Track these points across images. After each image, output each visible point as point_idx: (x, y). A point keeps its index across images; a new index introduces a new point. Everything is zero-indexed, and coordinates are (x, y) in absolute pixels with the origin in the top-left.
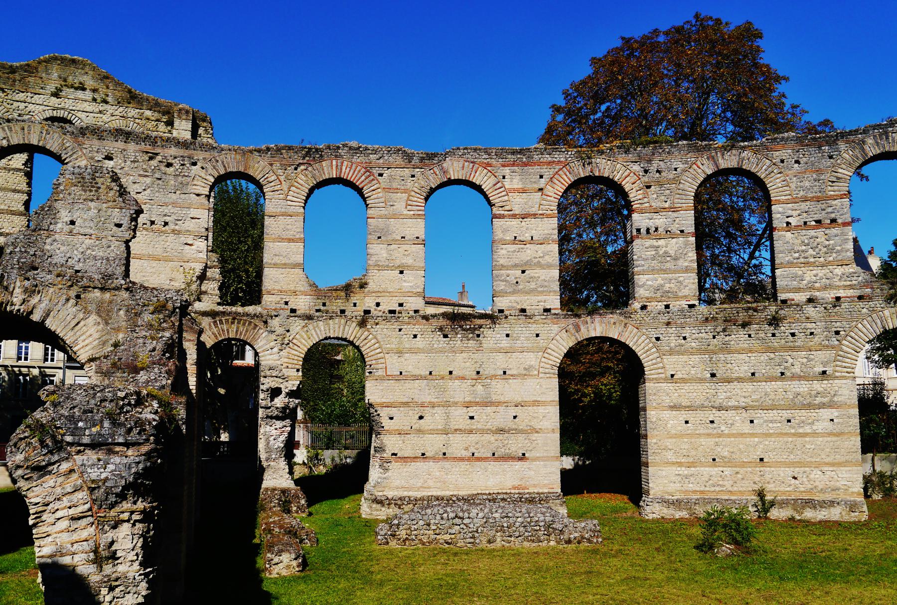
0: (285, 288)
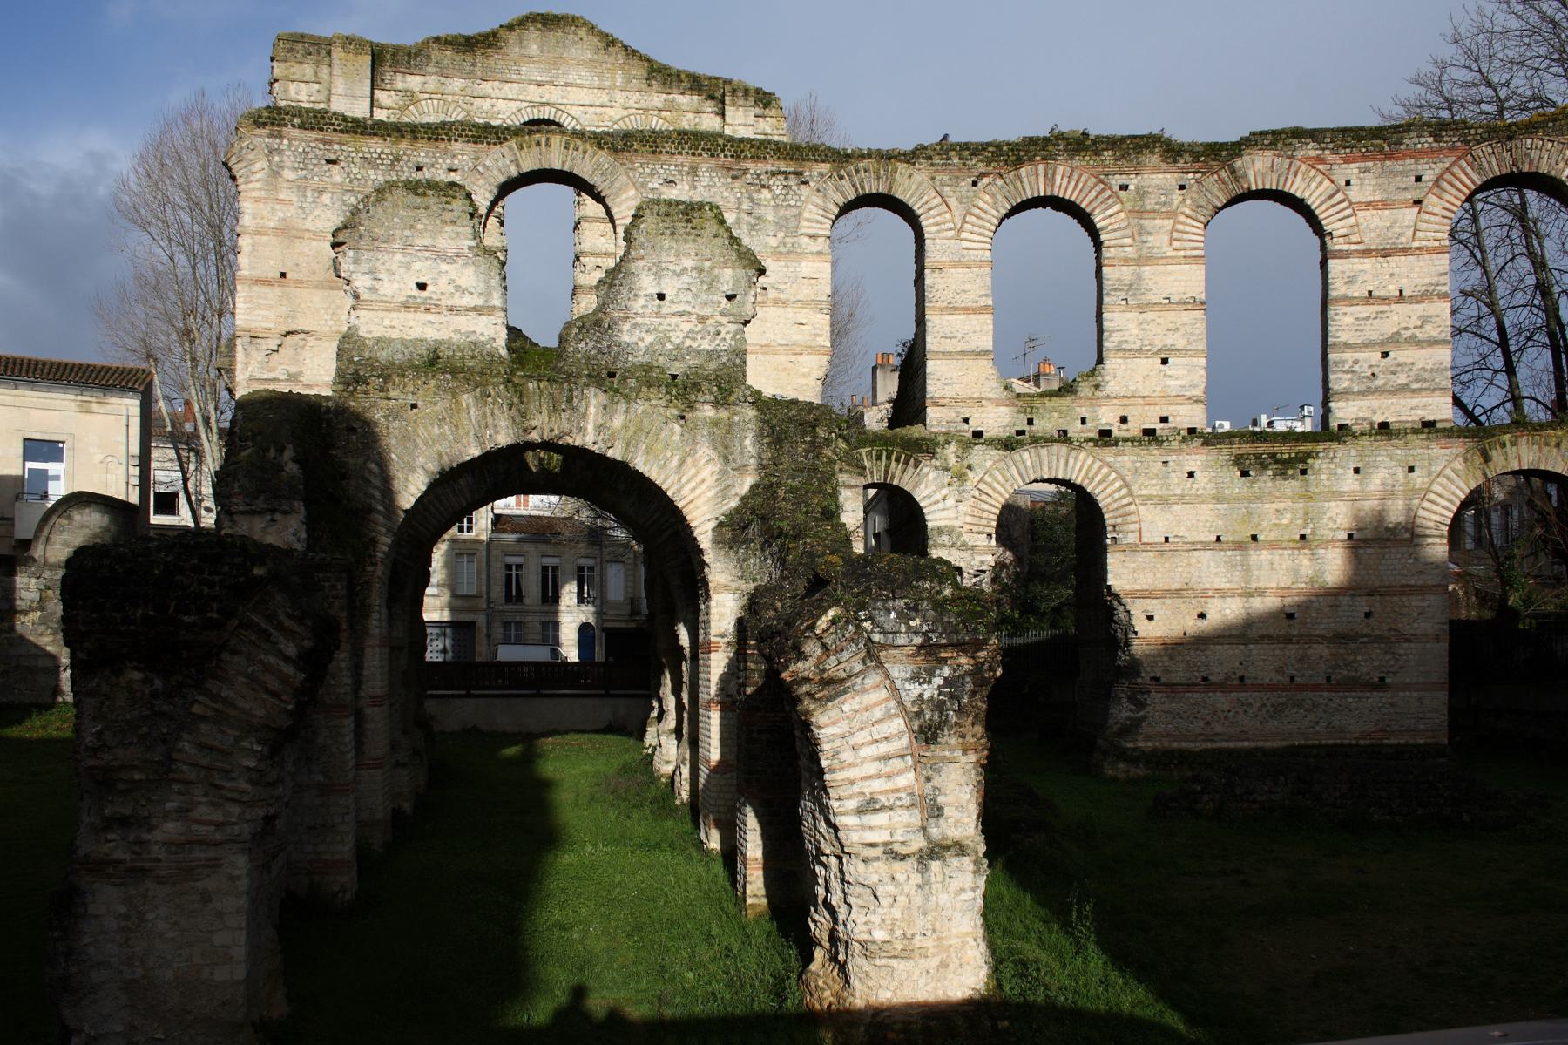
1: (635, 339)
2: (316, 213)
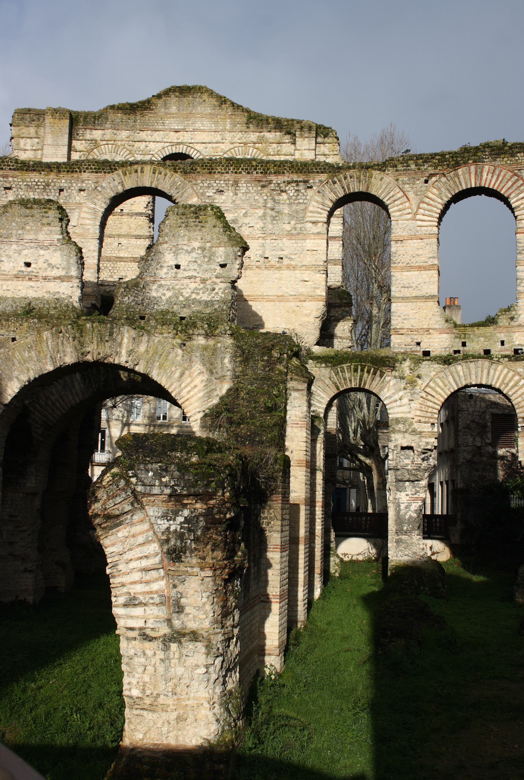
0: (416, 326)
1: (159, 294)
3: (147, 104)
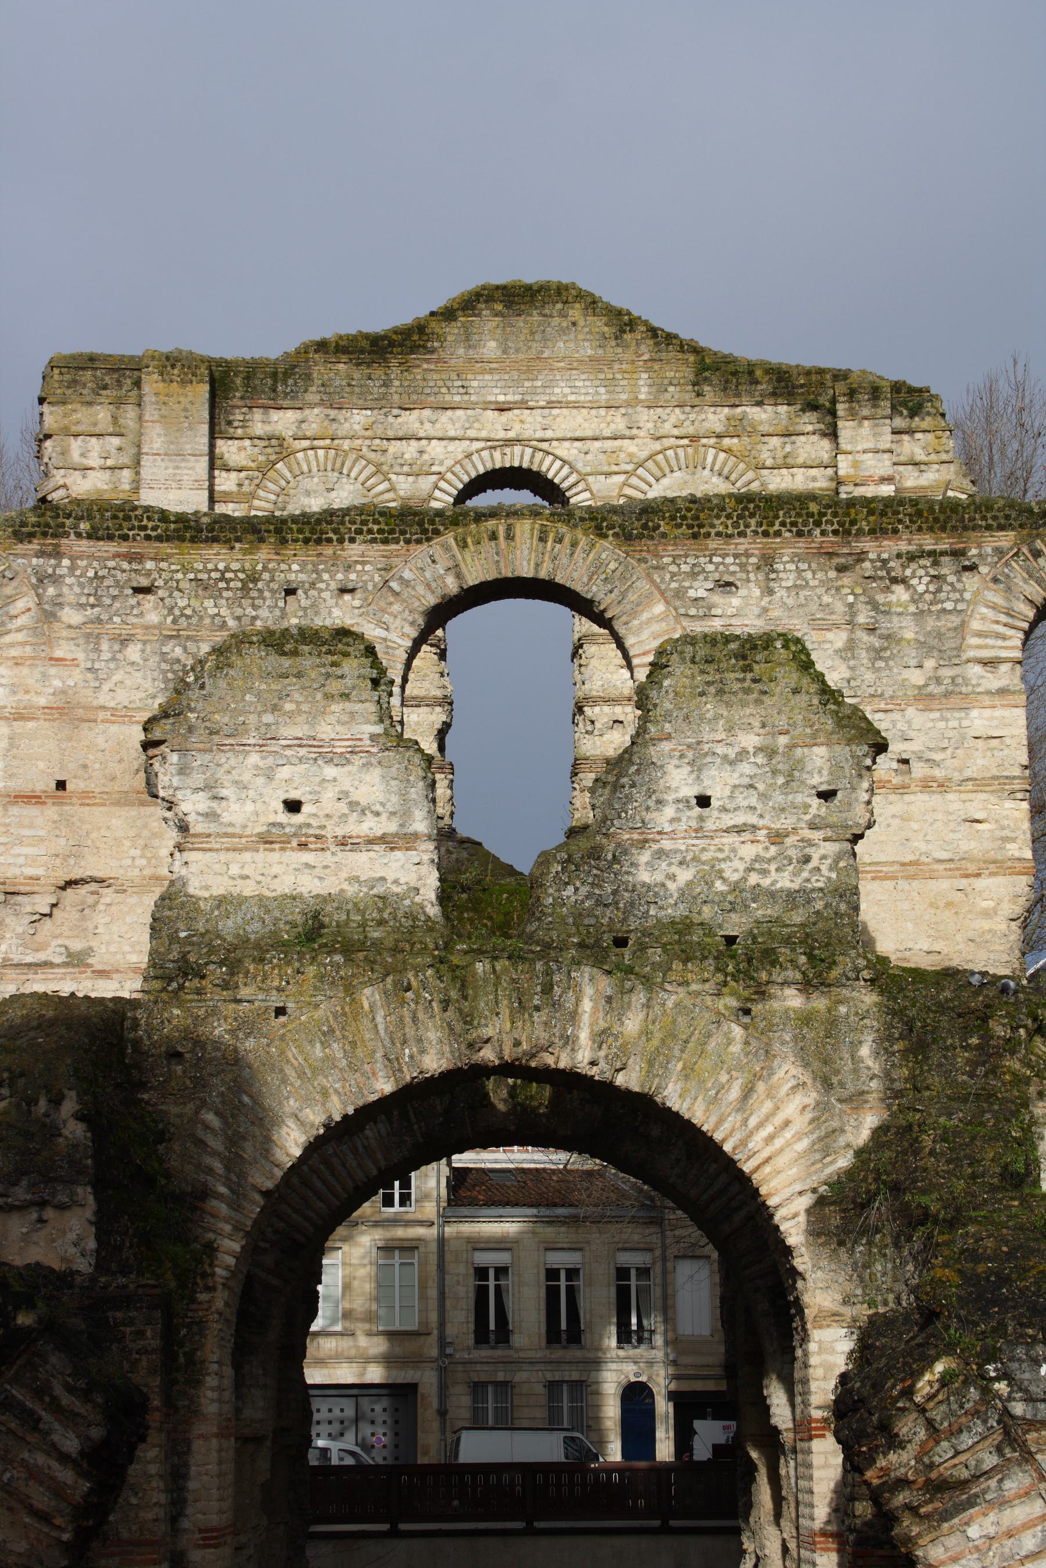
1: (659, 877)
2: (117, 677)
3: (415, 337)
